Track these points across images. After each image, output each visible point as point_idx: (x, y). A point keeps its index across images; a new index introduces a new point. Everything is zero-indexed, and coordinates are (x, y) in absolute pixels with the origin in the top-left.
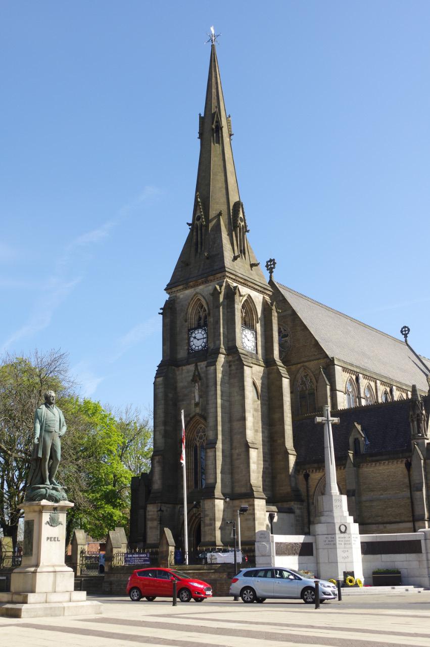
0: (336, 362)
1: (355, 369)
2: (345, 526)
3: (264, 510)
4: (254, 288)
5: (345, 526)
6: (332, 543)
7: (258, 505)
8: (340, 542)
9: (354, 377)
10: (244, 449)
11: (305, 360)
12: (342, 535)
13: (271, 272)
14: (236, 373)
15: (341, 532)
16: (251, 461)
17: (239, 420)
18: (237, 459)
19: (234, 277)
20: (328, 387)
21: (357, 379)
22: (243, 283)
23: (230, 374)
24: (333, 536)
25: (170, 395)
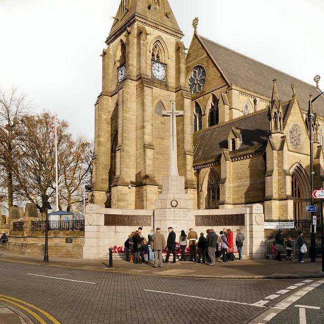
0: (233, 87)
1: (253, 94)
2: (176, 201)
3: (156, 194)
4: (165, 31)
5: (176, 201)
6: (163, 215)
7: (150, 190)
8: (170, 215)
9: (252, 100)
10: (142, 150)
11: (214, 89)
12: (173, 209)
13: (195, 28)
14: (140, 94)
15: (173, 206)
16: (147, 158)
17: (140, 129)
18: (139, 157)
19: (144, 21)
20: (227, 107)
21: (255, 101)
22: (154, 27)
23: (137, 95)
24: (165, 210)
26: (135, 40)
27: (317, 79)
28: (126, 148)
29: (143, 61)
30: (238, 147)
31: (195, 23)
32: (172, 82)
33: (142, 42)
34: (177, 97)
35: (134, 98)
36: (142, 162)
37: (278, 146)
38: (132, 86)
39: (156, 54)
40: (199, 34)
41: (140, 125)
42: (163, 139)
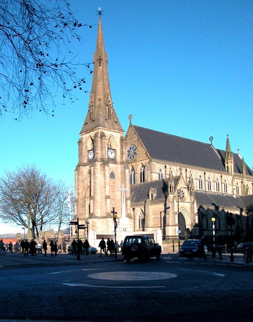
16: (107, 204)
25: (80, 178)
26: (99, 139)
27: (211, 139)
28: (96, 198)
29: (104, 151)
30: (154, 198)
31: (130, 117)
32: (119, 159)
33: (103, 141)
34: (121, 168)
35: (99, 171)
36: (104, 206)
37: (171, 200)
38: (98, 164)
39: (109, 144)
40: (132, 124)
41: (103, 186)
42: (114, 191)
